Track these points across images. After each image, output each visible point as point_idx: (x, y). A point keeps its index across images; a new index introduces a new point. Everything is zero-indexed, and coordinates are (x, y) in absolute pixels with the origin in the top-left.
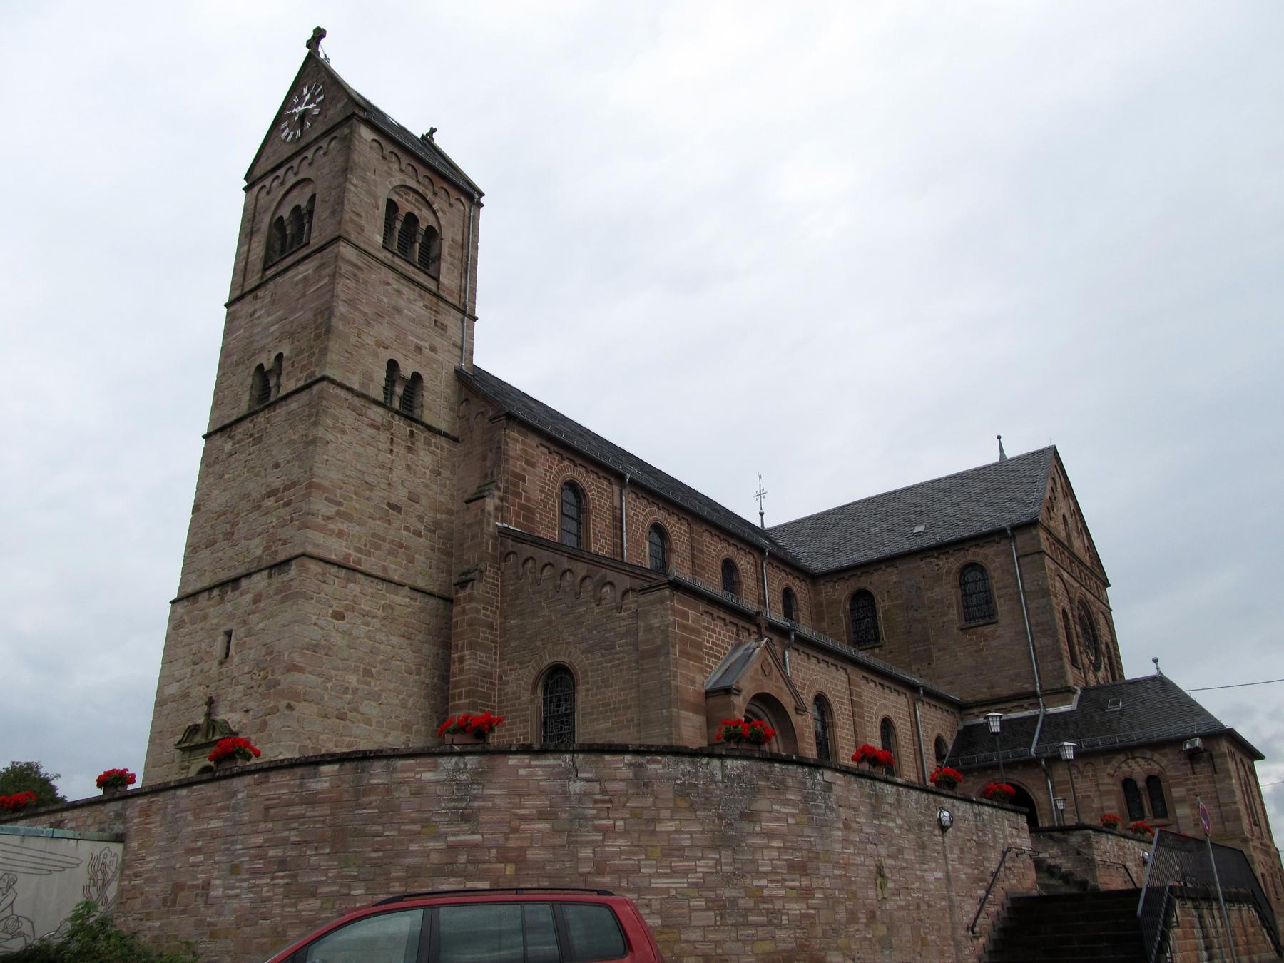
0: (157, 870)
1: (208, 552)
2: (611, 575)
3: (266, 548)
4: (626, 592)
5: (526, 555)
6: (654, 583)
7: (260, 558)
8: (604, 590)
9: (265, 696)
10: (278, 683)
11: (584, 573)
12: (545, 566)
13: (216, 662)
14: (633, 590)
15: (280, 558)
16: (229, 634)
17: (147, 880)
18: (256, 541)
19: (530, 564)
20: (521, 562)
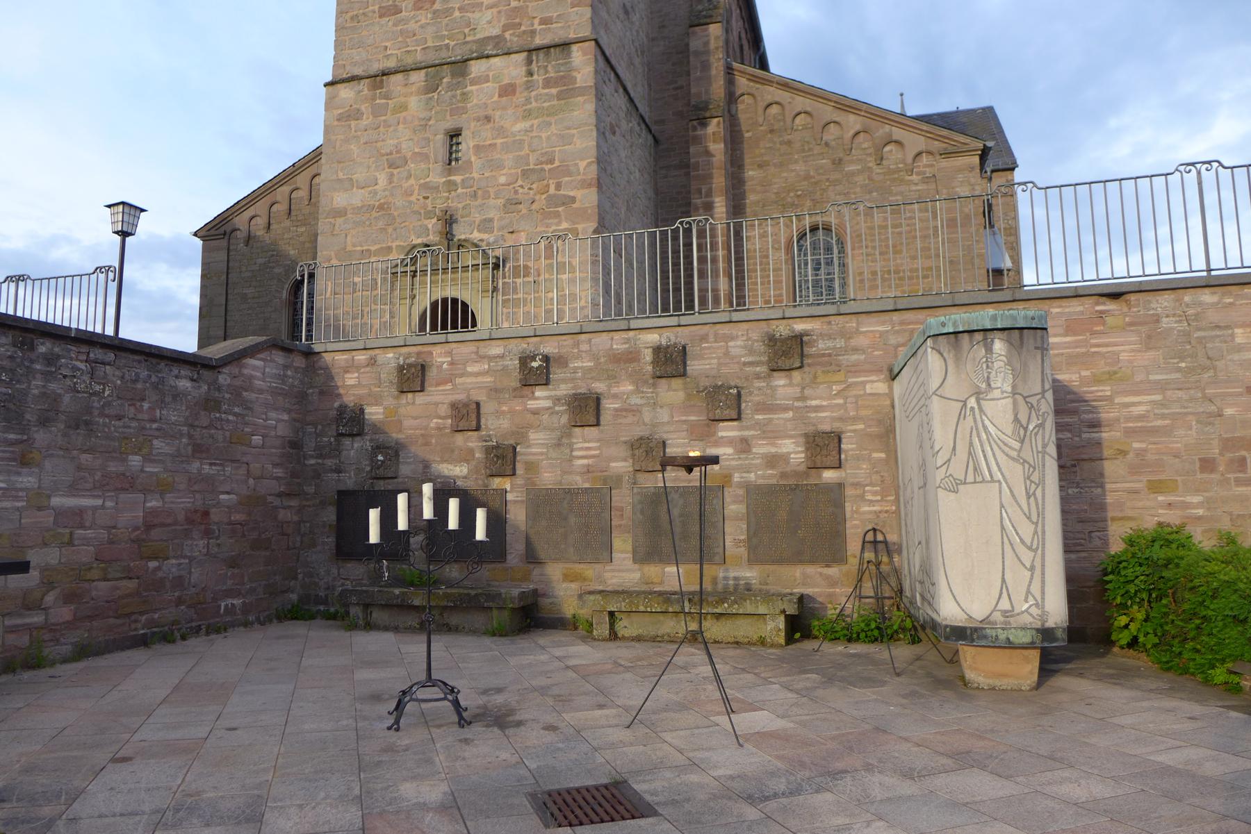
0: (1163, 417)
1: (388, 22)
2: (898, 133)
3: (505, 28)
4: (919, 154)
5: (769, 99)
6: (965, 148)
7: (498, 40)
8: (887, 148)
9: (546, 215)
10: (573, 199)
11: (858, 127)
12: (799, 114)
13: (439, 167)
14: (930, 153)
15: (538, 41)
16: (454, 135)
17: (1130, 432)
18: (488, 15)
19: (774, 110)
20: (762, 105)
